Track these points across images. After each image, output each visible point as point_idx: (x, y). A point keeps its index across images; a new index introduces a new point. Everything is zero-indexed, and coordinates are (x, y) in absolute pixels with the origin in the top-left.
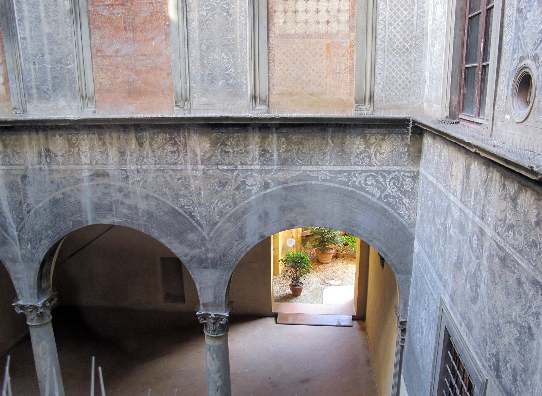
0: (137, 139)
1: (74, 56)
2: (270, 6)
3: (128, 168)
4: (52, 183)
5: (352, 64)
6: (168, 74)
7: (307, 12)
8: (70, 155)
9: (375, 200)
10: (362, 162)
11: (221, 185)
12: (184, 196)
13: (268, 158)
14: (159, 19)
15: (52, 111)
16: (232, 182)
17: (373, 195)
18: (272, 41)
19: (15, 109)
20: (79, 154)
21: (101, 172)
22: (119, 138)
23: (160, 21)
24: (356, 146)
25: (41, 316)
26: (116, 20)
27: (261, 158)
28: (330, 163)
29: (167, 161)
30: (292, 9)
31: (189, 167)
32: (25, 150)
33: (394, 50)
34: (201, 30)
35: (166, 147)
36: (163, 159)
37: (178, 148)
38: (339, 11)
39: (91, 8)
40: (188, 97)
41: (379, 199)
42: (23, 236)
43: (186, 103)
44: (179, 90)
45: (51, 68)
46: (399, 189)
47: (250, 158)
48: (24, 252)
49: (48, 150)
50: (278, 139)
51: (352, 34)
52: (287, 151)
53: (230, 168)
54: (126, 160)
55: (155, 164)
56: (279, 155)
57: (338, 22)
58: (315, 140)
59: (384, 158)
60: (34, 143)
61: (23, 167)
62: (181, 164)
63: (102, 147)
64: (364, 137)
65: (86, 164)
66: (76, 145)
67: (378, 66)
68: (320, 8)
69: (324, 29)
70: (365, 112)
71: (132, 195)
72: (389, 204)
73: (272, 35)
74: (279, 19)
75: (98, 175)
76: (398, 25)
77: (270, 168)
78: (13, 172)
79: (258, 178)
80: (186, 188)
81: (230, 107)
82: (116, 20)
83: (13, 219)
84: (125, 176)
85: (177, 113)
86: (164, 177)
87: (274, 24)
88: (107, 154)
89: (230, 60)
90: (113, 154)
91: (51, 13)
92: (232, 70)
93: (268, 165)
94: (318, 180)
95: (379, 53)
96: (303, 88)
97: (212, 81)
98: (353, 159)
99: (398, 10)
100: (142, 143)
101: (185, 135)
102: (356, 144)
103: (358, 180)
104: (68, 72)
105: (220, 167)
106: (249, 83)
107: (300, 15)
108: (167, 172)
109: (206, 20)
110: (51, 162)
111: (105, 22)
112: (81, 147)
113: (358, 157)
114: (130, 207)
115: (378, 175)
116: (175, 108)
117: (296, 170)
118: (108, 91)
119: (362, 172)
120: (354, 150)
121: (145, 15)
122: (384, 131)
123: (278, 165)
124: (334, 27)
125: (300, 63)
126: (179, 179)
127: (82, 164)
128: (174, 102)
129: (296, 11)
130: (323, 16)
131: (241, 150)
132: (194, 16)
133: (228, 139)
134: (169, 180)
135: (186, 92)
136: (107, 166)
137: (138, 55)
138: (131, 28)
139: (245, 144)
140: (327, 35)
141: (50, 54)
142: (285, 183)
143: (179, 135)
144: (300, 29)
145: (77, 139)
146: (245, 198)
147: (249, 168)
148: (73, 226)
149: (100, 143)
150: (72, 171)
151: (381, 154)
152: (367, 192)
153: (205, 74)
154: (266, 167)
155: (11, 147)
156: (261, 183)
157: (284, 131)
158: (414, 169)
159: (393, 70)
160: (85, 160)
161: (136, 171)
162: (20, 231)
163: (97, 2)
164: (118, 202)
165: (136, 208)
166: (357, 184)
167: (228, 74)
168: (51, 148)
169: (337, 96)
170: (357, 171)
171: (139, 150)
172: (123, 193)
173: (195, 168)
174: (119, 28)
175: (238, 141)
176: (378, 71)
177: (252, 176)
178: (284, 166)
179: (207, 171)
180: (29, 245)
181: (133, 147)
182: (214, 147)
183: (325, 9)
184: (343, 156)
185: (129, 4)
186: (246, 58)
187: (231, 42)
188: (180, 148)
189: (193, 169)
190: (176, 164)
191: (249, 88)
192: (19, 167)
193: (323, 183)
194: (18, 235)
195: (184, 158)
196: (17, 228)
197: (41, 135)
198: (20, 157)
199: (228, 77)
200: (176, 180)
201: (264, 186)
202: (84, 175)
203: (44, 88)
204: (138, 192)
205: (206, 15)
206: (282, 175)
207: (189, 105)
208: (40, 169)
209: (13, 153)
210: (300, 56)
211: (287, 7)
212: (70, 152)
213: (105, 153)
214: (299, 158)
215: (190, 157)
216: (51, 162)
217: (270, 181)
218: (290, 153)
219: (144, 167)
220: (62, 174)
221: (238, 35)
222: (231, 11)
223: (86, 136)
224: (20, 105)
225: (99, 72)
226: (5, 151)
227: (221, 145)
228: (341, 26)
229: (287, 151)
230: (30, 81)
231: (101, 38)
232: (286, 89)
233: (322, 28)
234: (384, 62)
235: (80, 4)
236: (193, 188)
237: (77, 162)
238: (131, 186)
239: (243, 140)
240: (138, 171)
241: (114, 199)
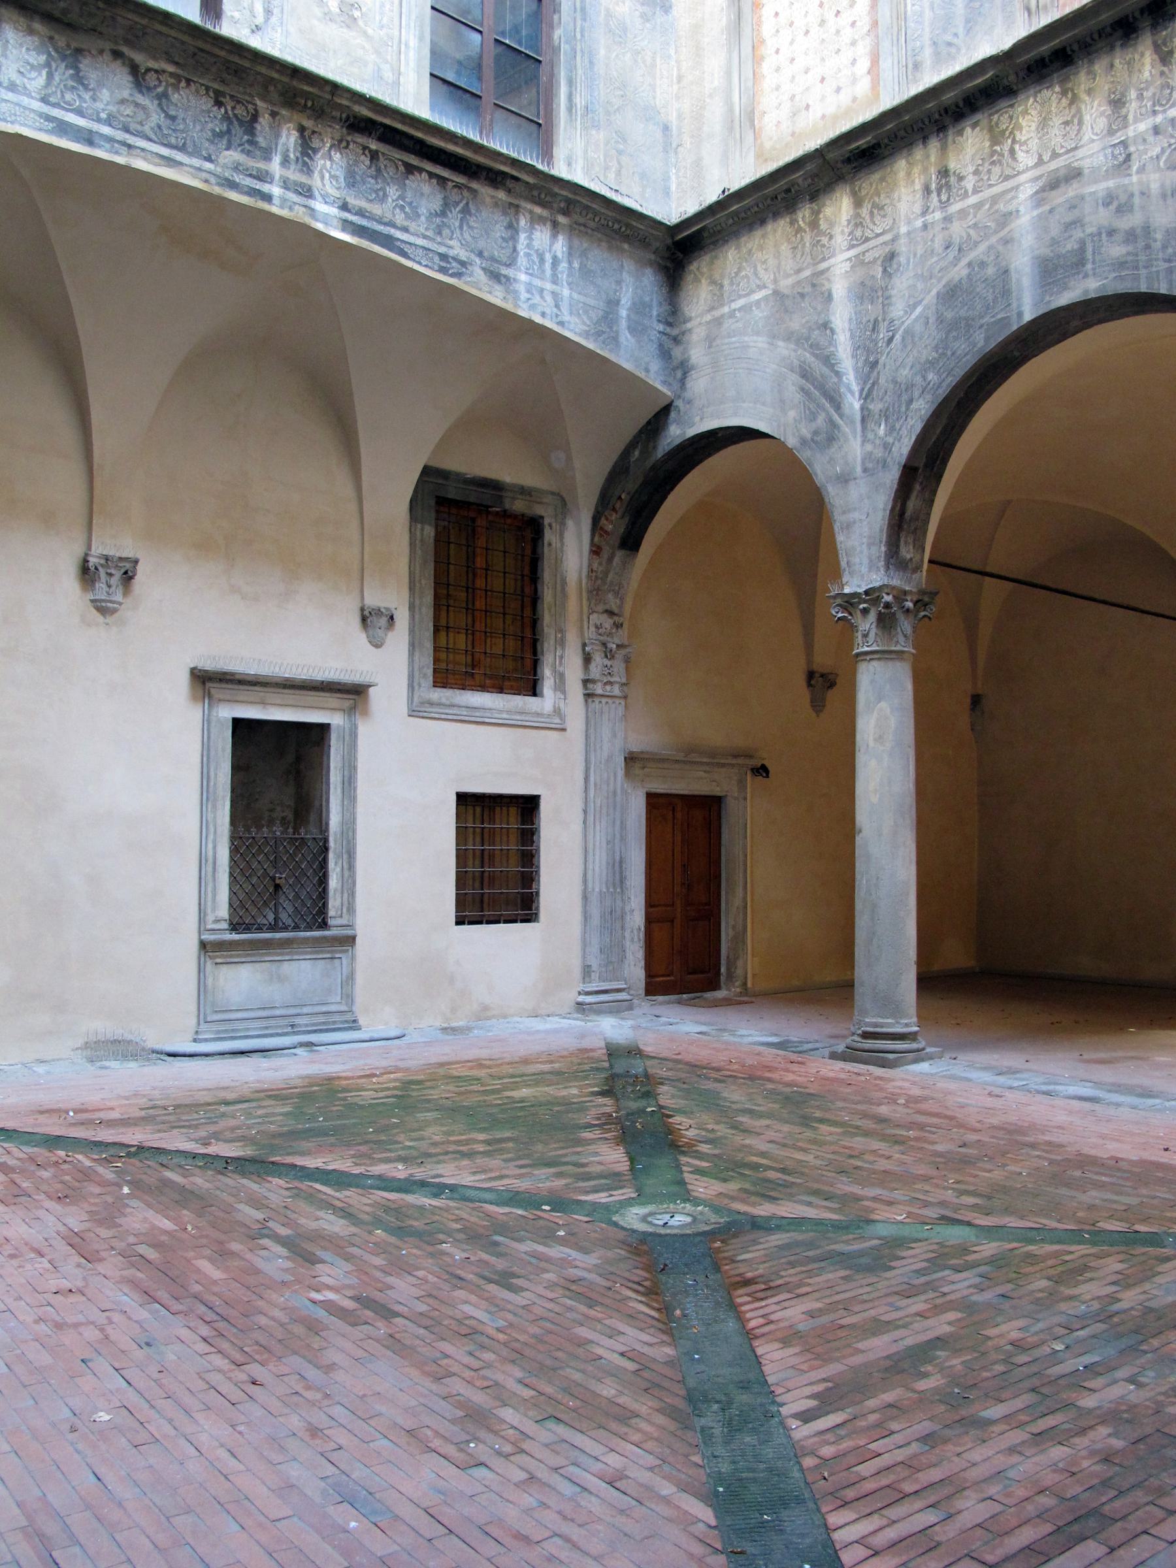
20: (1012, 152)
21: (1062, 173)
25: (886, 622)
32: (896, 195)
42: (871, 407)
48: (869, 447)
49: (944, 173)
60: (916, 170)
63: (1067, 111)
65: (1028, 169)
66: (1007, 133)
71: (1137, 200)
75: (1054, 183)
78: (868, 257)
83: (856, 370)
88: (1080, 123)
110: (949, 199)
112: (1017, 133)
114: (1130, 236)
127: (1019, 173)
145: (1011, 118)
148: (987, 339)
149: (1065, 102)
150: (994, 199)
160: (1025, 159)
162: (866, 396)
164: (1100, 234)
165: (1147, 229)
168: (952, 165)
172: (1113, 207)
180: (882, 427)
192: (881, 239)
194: (862, 409)
196: (863, 389)
198: (884, 216)
204: (1155, 187)
208: (925, 227)
209: (872, 213)
216: (949, 199)
220: (971, 216)
226: (858, 215)
237: (1008, 172)
241: (1089, 230)
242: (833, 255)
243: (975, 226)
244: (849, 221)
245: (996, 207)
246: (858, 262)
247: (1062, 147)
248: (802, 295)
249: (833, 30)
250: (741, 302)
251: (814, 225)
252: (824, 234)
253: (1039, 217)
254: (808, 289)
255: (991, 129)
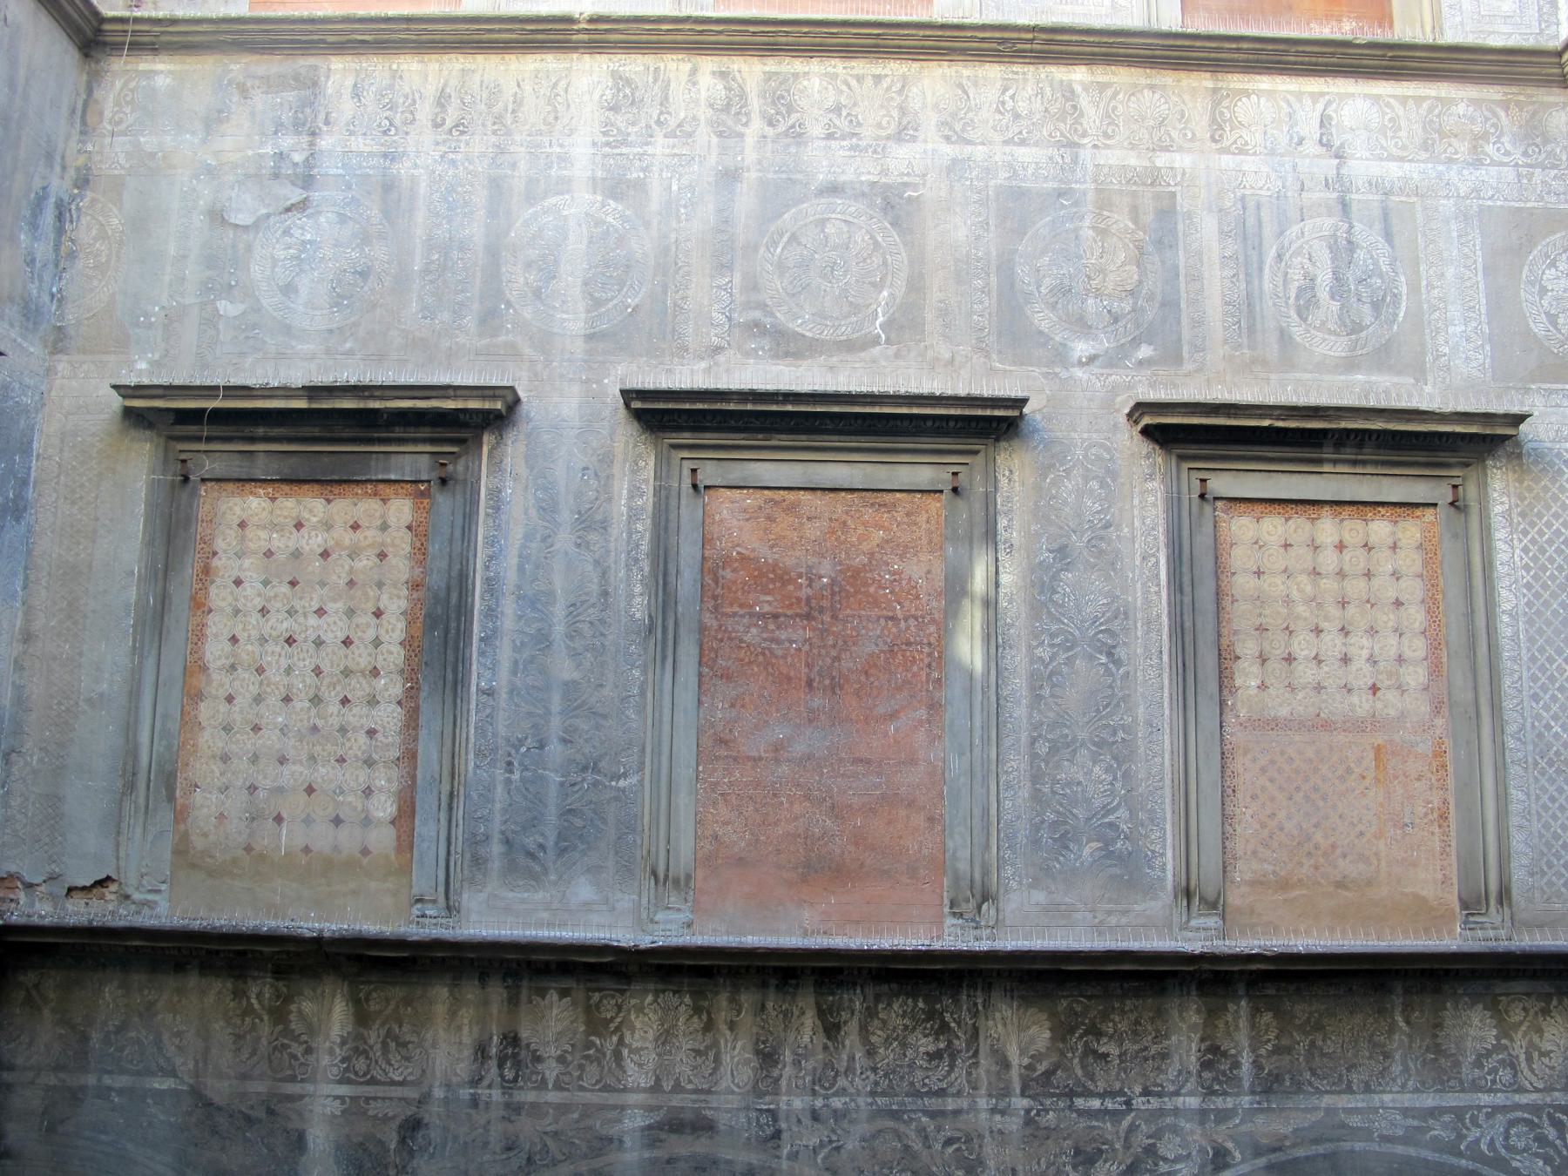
0: (821, 1013)
1: (643, 750)
2: (1225, 641)
3: (783, 1107)
4: (509, 1149)
5: (1445, 802)
6: (931, 819)
7: (1320, 662)
8: (587, 1057)
10: (1494, 1082)
11: (1080, 1159)
13: (1224, 1074)
14: (914, 661)
15: (546, 915)
16: (1114, 1150)
18: (1232, 735)
19: (418, 901)
20: (617, 1055)
21: (688, 1116)
22: (763, 1007)
23: (915, 668)
24: (1472, 1032)
26: (784, 657)
27: (1207, 1075)
28: (1404, 1086)
29: (912, 1084)
30: (1280, 652)
31: (983, 1103)
32: (429, 1036)
33: (1551, 763)
34: (1037, 699)
35: (911, 1039)
36: (902, 1078)
37: (950, 1042)
38: (1400, 659)
39: (709, 619)
40: (994, 888)
43: (985, 906)
44: (963, 866)
45: (562, 784)
47: (1172, 1073)
49: (512, 1039)
50: (1253, 1016)
51: (1439, 722)
52: (1277, 1050)
53: (1110, 1106)
54: (777, 1080)
55: (873, 1094)
56: (1257, 1065)
57: (1401, 689)
58: (1358, 1019)
59: (1553, 1068)
60: (466, 1015)
61: (412, 1093)
62: (959, 1094)
63: (700, 1037)
64: (1493, 1006)
65: (638, 1090)
66: (612, 1026)
67: (1513, 807)
68: (1353, 651)
69: (1366, 706)
70: (1491, 933)
73: (1230, 719)
74: (1247, 677)
75: (676, 1125)
76: (1554, 698)
77: (1230, 1103)
78: (374, 1109)
79: (1196, 1136)
81: (1113, 920)
82: (784, 657)
84: (769, 1131)
85: (954, 937)
86: (899, 1136)
87: (1234, 690)
89: (1118, 785)
90: (737, 1057)
91: (585, 627)
92: (1122, 813)
93: (1225, 1093)
94: (1369, 1139)
95: (1514, 770)
96: (1316, 868)
97: (1064, 842)
98: (1468, 1072)
99: (1550, 660)
100: (837, 1027)
101: (976, 1004)
102: (1474, 1029)
104: (617, 799)
105: (1079, 1102)
106: (1169, 853)
107: (1301, 667)
108: (911, 1120)
109: (1052, 674)
110: (515, 1080)
111: (750, 663)
112: (627, 1034)
113: (1481, 1066)
115: (1540, 1118)
116: (950, 921)
117: (1306, 1110)
118: (741, 861)
119: (1497, 1109)
120: (1469, 1044)
121: (871, 648)
122: (1545, 987)
123: (1253, 1093)
124: (1391, 703)
125: (1307, 798)
126: (949, 1142)
127: (625, 1090)
128: (946, 902)
129: (1290, 659)
130: (1361, 673)
131: (1146, 1049)
132: (1017, 660)
133: (1105, 1016)
134: (917, 1145)
135: (986, 873)
136: (709, 1098)
137: (841, 760)
138: (827, 682)
139: (1157, 1031)
140: (1373, 722)
141: (564, 741)
142: (1274, 1150)
143: (957, 1002)
144: (1300, 705)
145: (620, 1008)
147: (1169, 1104)
150: (587, 1111)
151: (1543, 1054)
153: (1043, 822)
154: (1219, 1102)
155: (383, 1025)
156: (1202, 1150)
157: (1269, 992)
159: (1554, 817)
160: (637, 1075)
161: (808, 1115)
163: (731, 605)
166: (1484, 1147)
167: (1111, 825)
168: (524, 1034)
169: (1408, 890)
170: (1479, 1108)
171: (825, 1048)
173: (1002, 1105)
174: (789, 679)
175: (1137, 1022)
176: (1514, 820)
177: (1175, 1130)
178: (1272, 1097)
179: (1038, 1114)
181: (806, 1039)
182: (1064, 1040)
183: (1365, 653)
184: (1441, 1067)
185: (827, 618)
186: (1162, 779)
187: (1121, 734)
188: (956, 1042)
189: (993, 1111)
190: (941, 1093)
191: (1169, 867)
193: (1387, 1148)
195: (969, 1074)
197: (497, 992)
198: (407, 1059)
199: (1111, 834)
200: (938, 1147)
201: (1213, 1161)
202: (628, 1124)
203: (530, 841)
205: (1052, 659)
206: (1270, 1126)
207: (993, 912)
208: (475, 1102)
209: (385, 1044)
210: (1306, 779)
211: (1267, 647)
212: (589, 1049)
213: (711, 1055)
214: (1314, 1074)
215: (988, 1071)
216: (515, 1080)
217: (1230, 1145)
218: (1287, 1058)
219: (837, 1103)
220: (549, 1120)
221: (1141, 718)
222: (1121, 652)
223: (650, 998)
224: (441, 889)
225: (715, 803)
226: (359, 1037)
227: (1086, 1033)
228: (1409, 700)
229: (1277, 1050)
230: (485, 819)
231: (732, 706)
232: (1271, 868)
233: (1361, 704)
234: (1528, 794)
235: (680, 609)
237: (610, 1081)
238: (785, 1165)
239: (1152, 1020)
240: (815, 1116)
242: (312, 1080)
243: (556, 1135)
244: (343, 1043)
245: (589, 1122)
246: (354, 1109)
247: (690, 1082)
248: (249, 1120)
249: (335, 722)
250: (123, 1081)
251: (279, 1015)
252: (296, 1038)
253: (653, 1162)
254: (260, 1113)
255: (588, 1010)
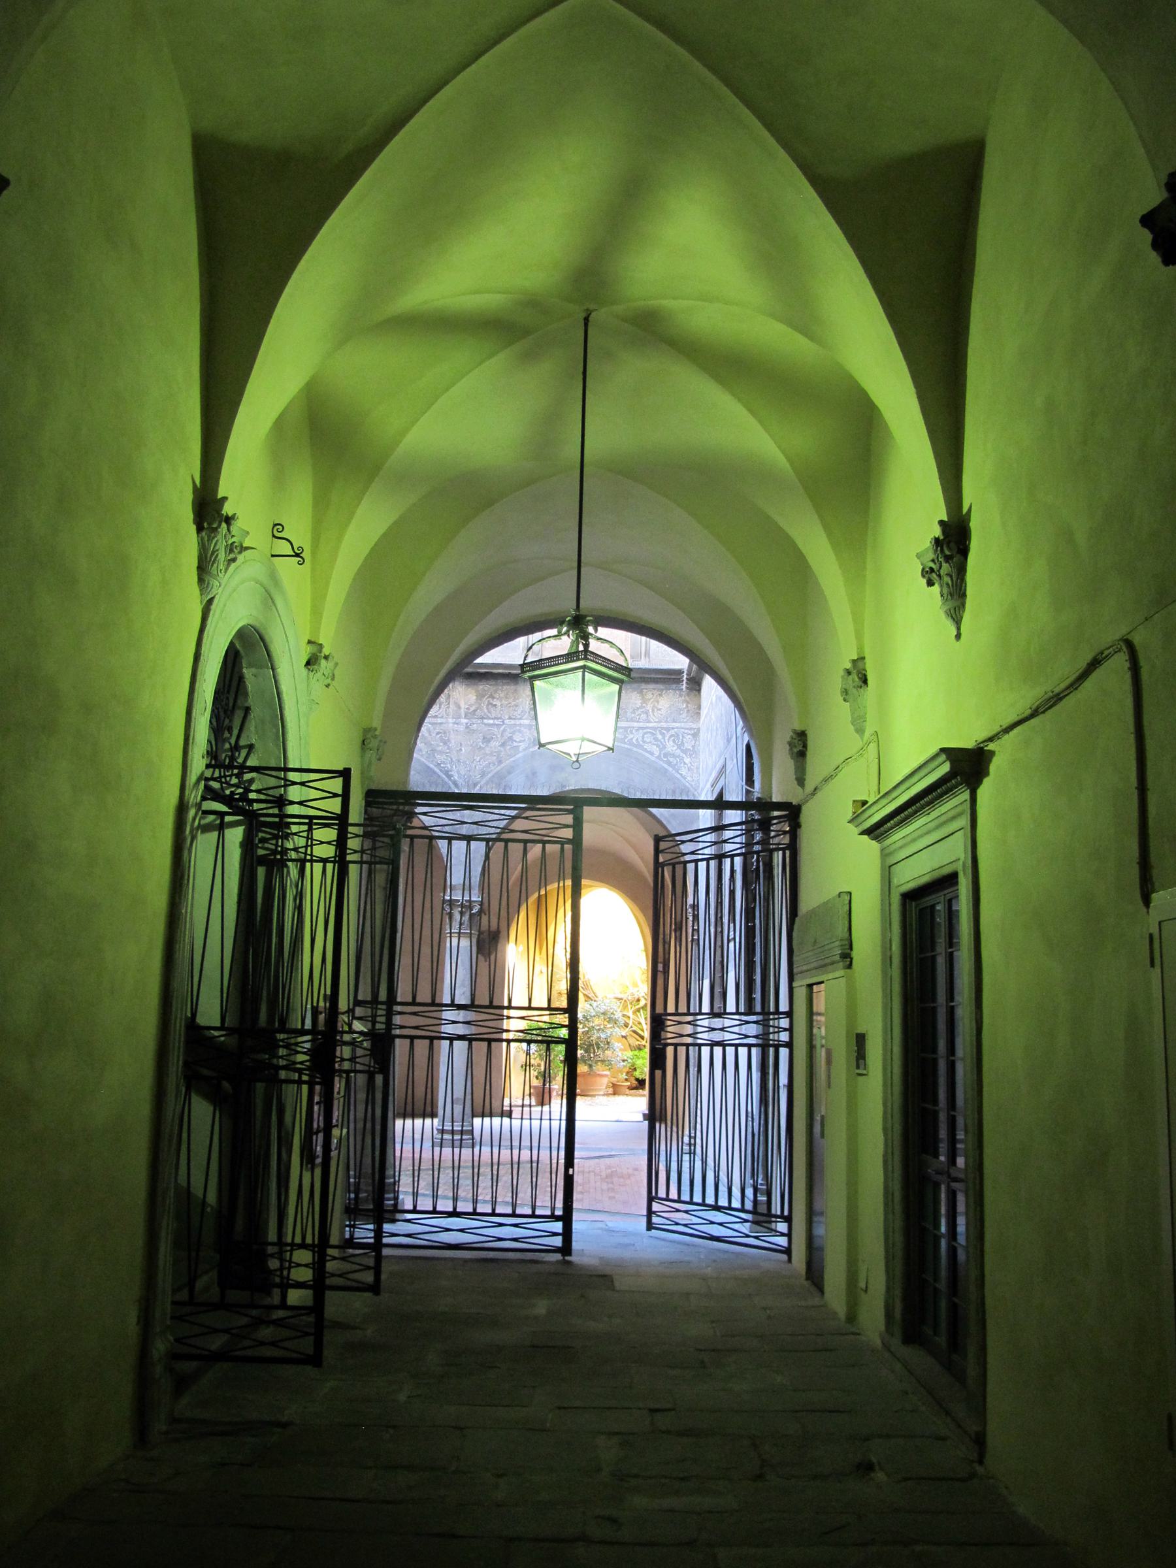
9: (653, 759)
12: (441, 753)
17: (652, 754)
41: (659, 757)
46: (679, 747)
64: (641, 692)
72: (669, 763)
80: (445, 743)
103: (636, 737)
122: (661, 686)
133: (496, 692)
146: (510, 756)
147: (518, 722)
152: (645, 750)
158: (694, 726)
236: (452, 744)
